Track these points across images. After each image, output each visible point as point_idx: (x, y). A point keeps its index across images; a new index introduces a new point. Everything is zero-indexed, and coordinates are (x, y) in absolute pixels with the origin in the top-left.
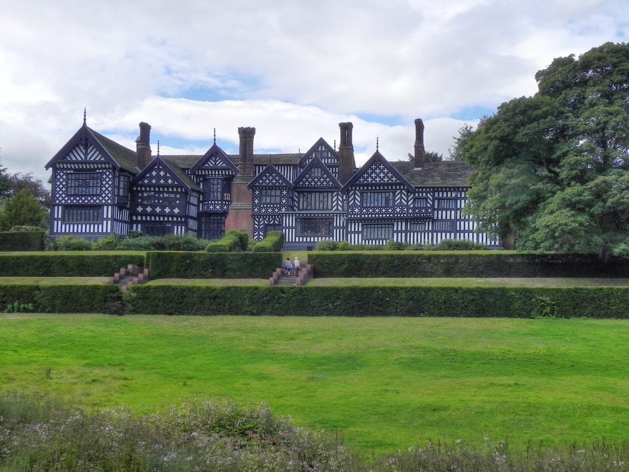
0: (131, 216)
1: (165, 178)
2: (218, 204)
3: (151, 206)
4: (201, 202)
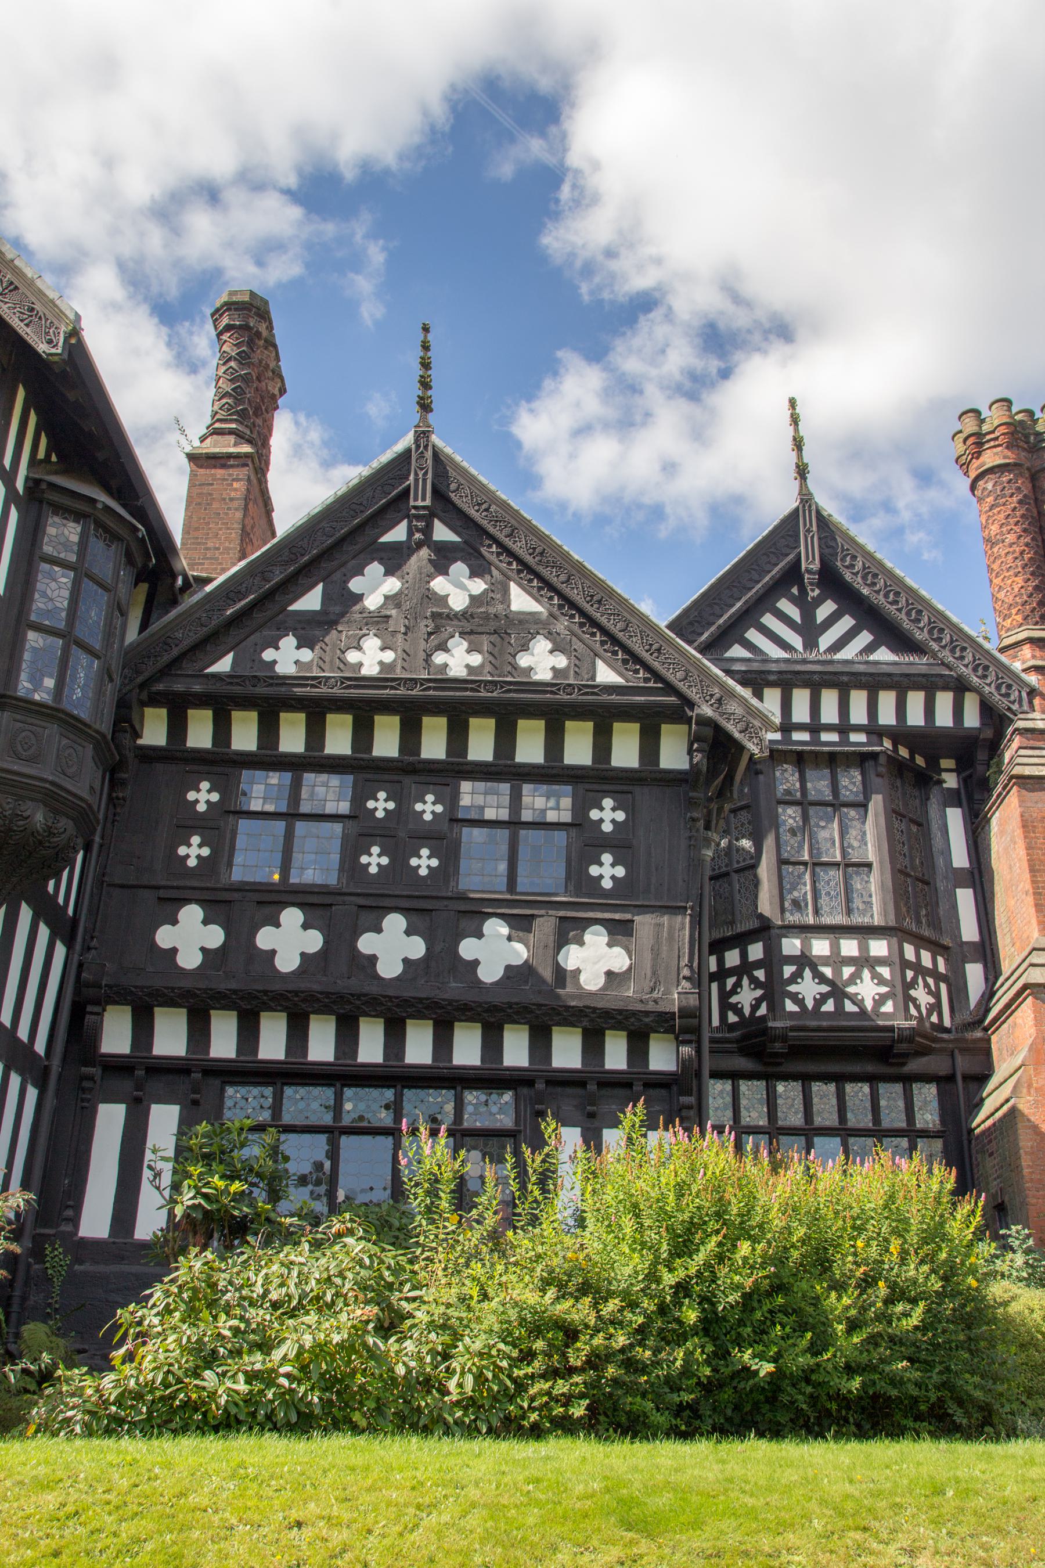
1: (487, 624)
2: (865, 961)
3: (316, 904)
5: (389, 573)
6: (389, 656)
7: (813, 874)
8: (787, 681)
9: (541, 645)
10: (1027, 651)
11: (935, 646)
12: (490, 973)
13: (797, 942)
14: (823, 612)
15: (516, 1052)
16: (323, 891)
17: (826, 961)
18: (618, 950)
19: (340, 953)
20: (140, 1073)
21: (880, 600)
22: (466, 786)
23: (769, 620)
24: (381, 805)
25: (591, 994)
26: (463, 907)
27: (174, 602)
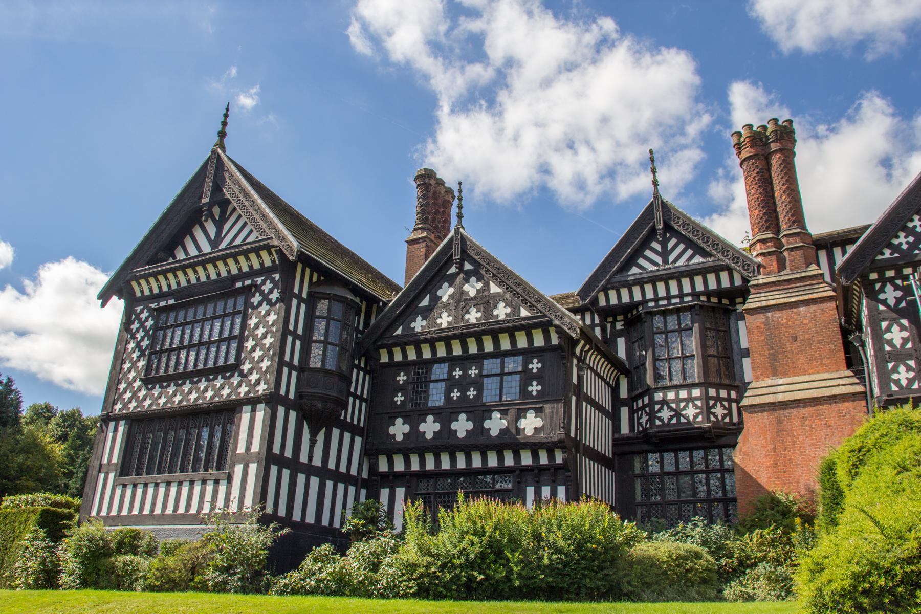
0: (370, 453)
2: (690, 399)
3: (437, 413)
4: (624, 403)
5: (450, 286)
6: (450, 319)
7: (669, 363)
8: (653, 280)
9: (502, 305)
10: (758, 246)
11: (714, 252)
12: (494, 433)
13: (661, 394)
14: (670, 245)
15: (509, 461)
16: (439, 408)
17: (673, 401)
18: (538, 419)
19: (446, 432)
20: (391, 478)
21: (690, 236)
22: (486, 362)
23: (648, 253)
24: (458, 373)
25: (529, 437)
26: (484, 409)
27: (382, 310)
